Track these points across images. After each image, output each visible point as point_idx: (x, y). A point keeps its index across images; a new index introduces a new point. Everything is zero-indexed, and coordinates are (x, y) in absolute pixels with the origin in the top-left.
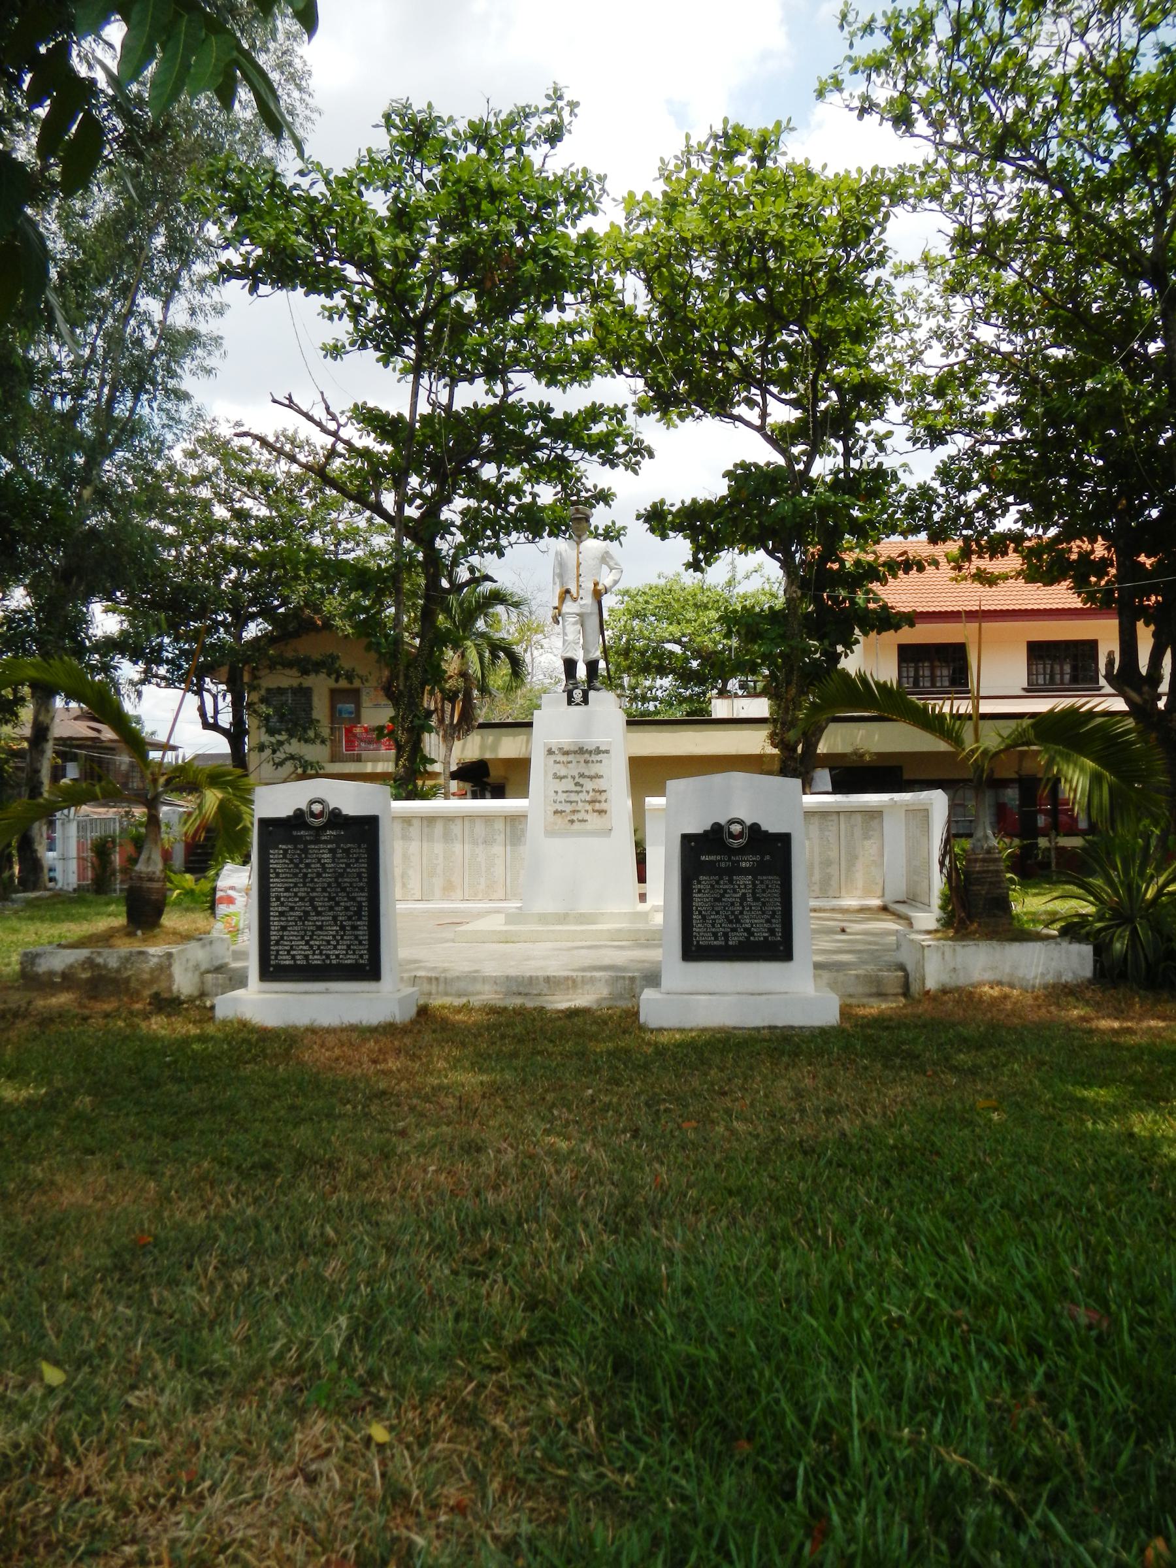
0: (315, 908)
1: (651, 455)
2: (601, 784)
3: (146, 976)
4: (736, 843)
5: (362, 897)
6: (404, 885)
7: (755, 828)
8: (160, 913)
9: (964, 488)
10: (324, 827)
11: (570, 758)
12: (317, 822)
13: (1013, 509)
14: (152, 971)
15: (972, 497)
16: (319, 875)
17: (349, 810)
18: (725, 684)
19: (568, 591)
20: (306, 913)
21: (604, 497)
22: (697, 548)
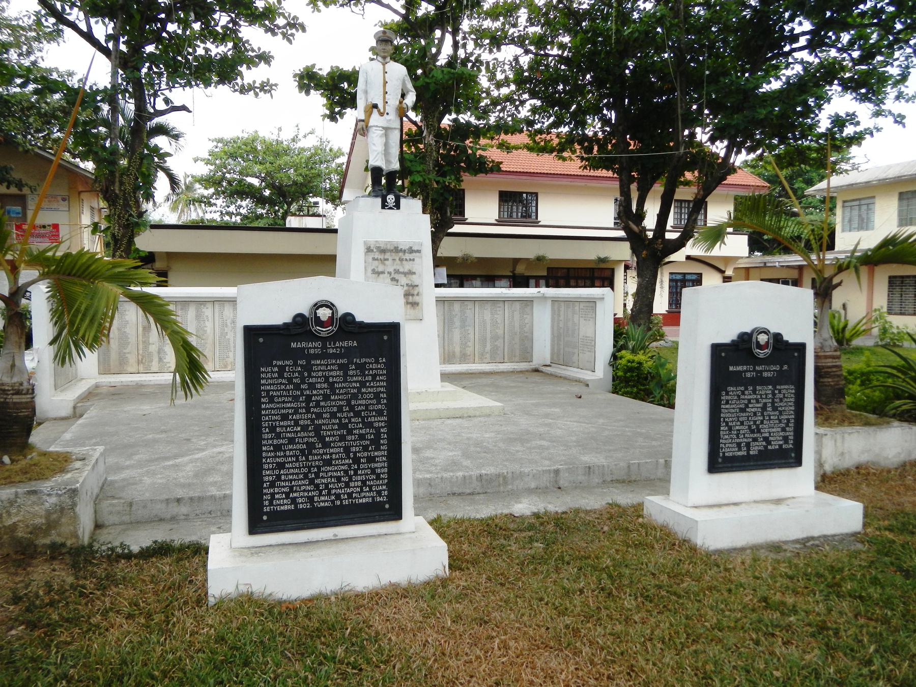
0: (322, 439)
1: (304, 30)
2: (415, 279)
3: (39, 521)
4: (761, 354)
5: (380, 422)
6: (160, 360)
7: (778, 337)
8: (28, 431)
9: (499, 85)
10: (333, 338)
11: (388, 255)
12: (324, 331)
13: (528, 103)
14: (49, 513)
15: (505, 91)
16: (326, 398)
17: (364, 315)
18: (289, 207)
19: (375, 106)
20: (311, 446)
21: (265, 58)
22: (331, 107)
